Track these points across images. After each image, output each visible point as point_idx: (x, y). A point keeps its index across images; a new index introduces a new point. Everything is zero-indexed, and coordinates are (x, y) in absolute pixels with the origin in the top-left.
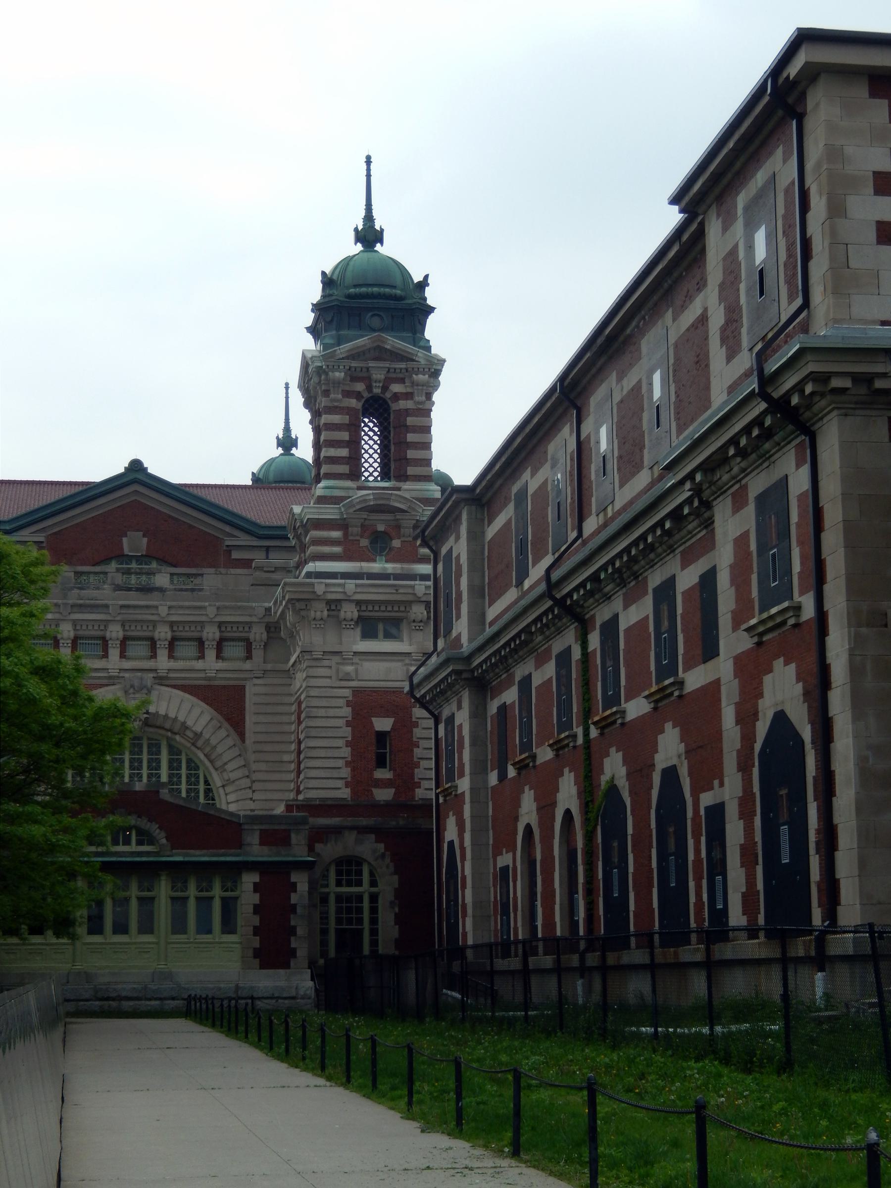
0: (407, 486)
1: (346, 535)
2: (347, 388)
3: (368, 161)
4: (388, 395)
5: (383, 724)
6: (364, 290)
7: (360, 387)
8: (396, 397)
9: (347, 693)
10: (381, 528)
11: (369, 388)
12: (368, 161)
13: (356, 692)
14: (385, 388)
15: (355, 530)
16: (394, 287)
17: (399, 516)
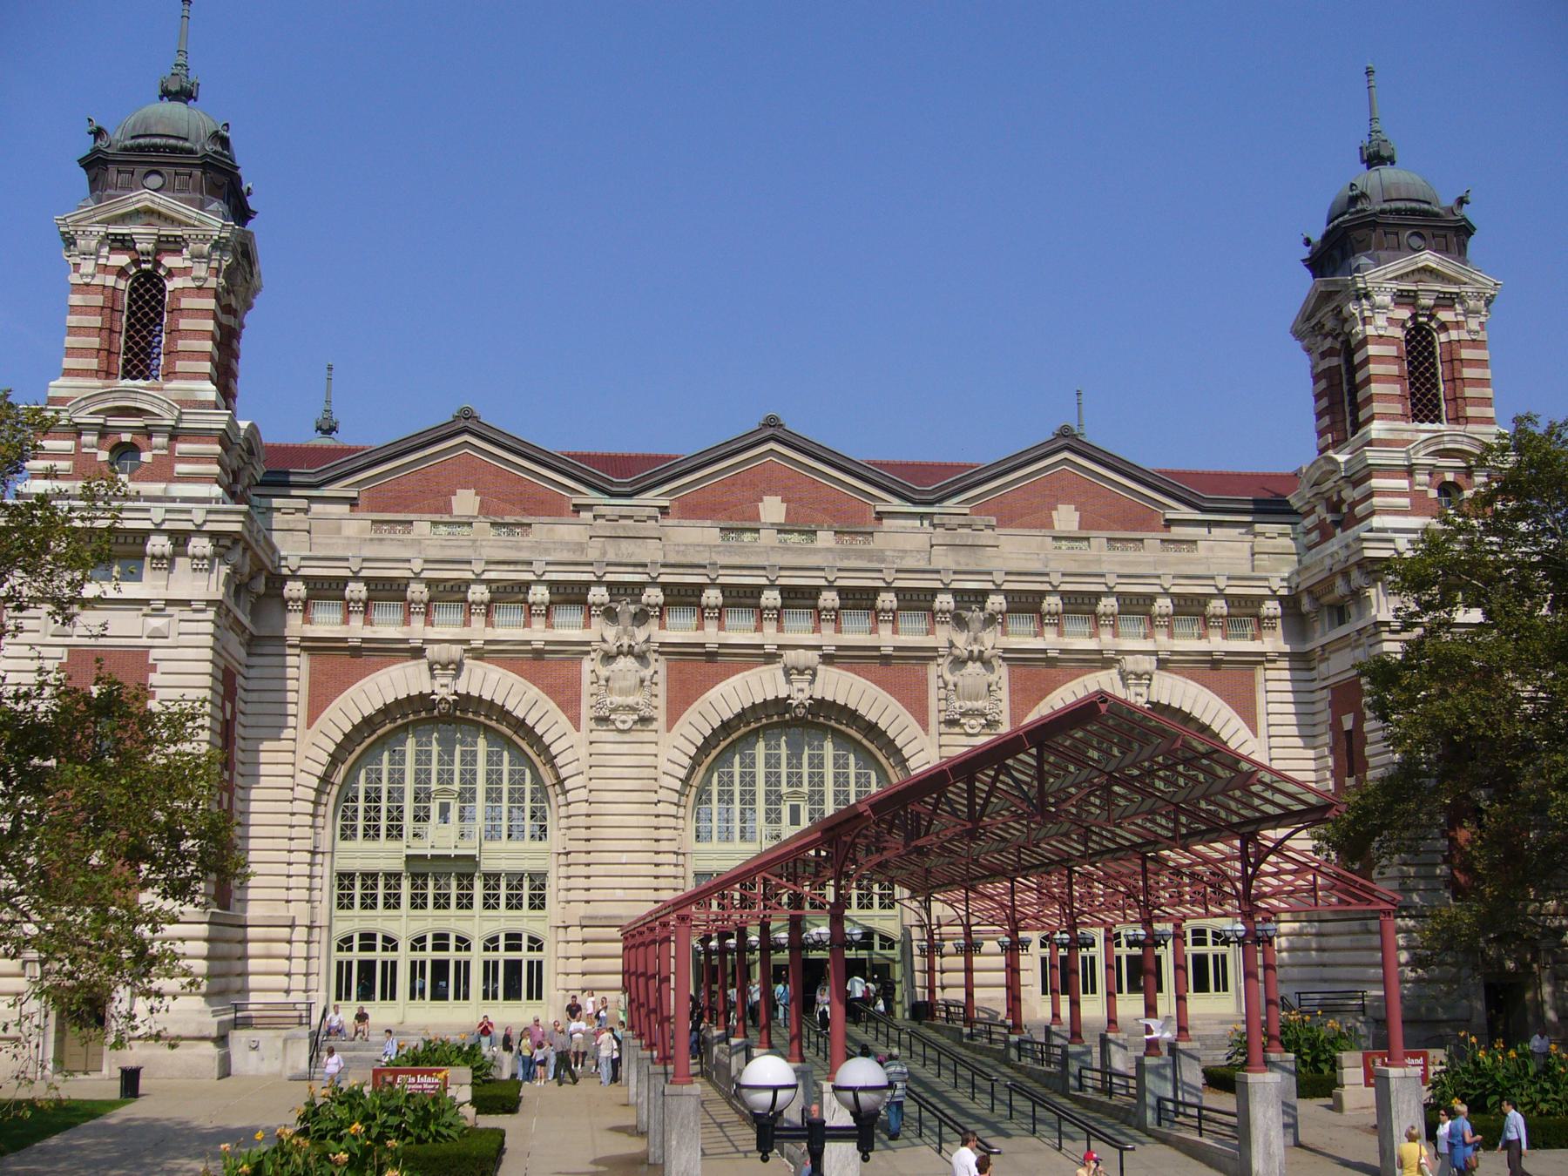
0: (175, 384)
1: (79, 446)
2: (102, 261)
6: (141, 141)
8: (171, 273)
10: (126, 437)
14: (158, 264)
16: (186, 139)
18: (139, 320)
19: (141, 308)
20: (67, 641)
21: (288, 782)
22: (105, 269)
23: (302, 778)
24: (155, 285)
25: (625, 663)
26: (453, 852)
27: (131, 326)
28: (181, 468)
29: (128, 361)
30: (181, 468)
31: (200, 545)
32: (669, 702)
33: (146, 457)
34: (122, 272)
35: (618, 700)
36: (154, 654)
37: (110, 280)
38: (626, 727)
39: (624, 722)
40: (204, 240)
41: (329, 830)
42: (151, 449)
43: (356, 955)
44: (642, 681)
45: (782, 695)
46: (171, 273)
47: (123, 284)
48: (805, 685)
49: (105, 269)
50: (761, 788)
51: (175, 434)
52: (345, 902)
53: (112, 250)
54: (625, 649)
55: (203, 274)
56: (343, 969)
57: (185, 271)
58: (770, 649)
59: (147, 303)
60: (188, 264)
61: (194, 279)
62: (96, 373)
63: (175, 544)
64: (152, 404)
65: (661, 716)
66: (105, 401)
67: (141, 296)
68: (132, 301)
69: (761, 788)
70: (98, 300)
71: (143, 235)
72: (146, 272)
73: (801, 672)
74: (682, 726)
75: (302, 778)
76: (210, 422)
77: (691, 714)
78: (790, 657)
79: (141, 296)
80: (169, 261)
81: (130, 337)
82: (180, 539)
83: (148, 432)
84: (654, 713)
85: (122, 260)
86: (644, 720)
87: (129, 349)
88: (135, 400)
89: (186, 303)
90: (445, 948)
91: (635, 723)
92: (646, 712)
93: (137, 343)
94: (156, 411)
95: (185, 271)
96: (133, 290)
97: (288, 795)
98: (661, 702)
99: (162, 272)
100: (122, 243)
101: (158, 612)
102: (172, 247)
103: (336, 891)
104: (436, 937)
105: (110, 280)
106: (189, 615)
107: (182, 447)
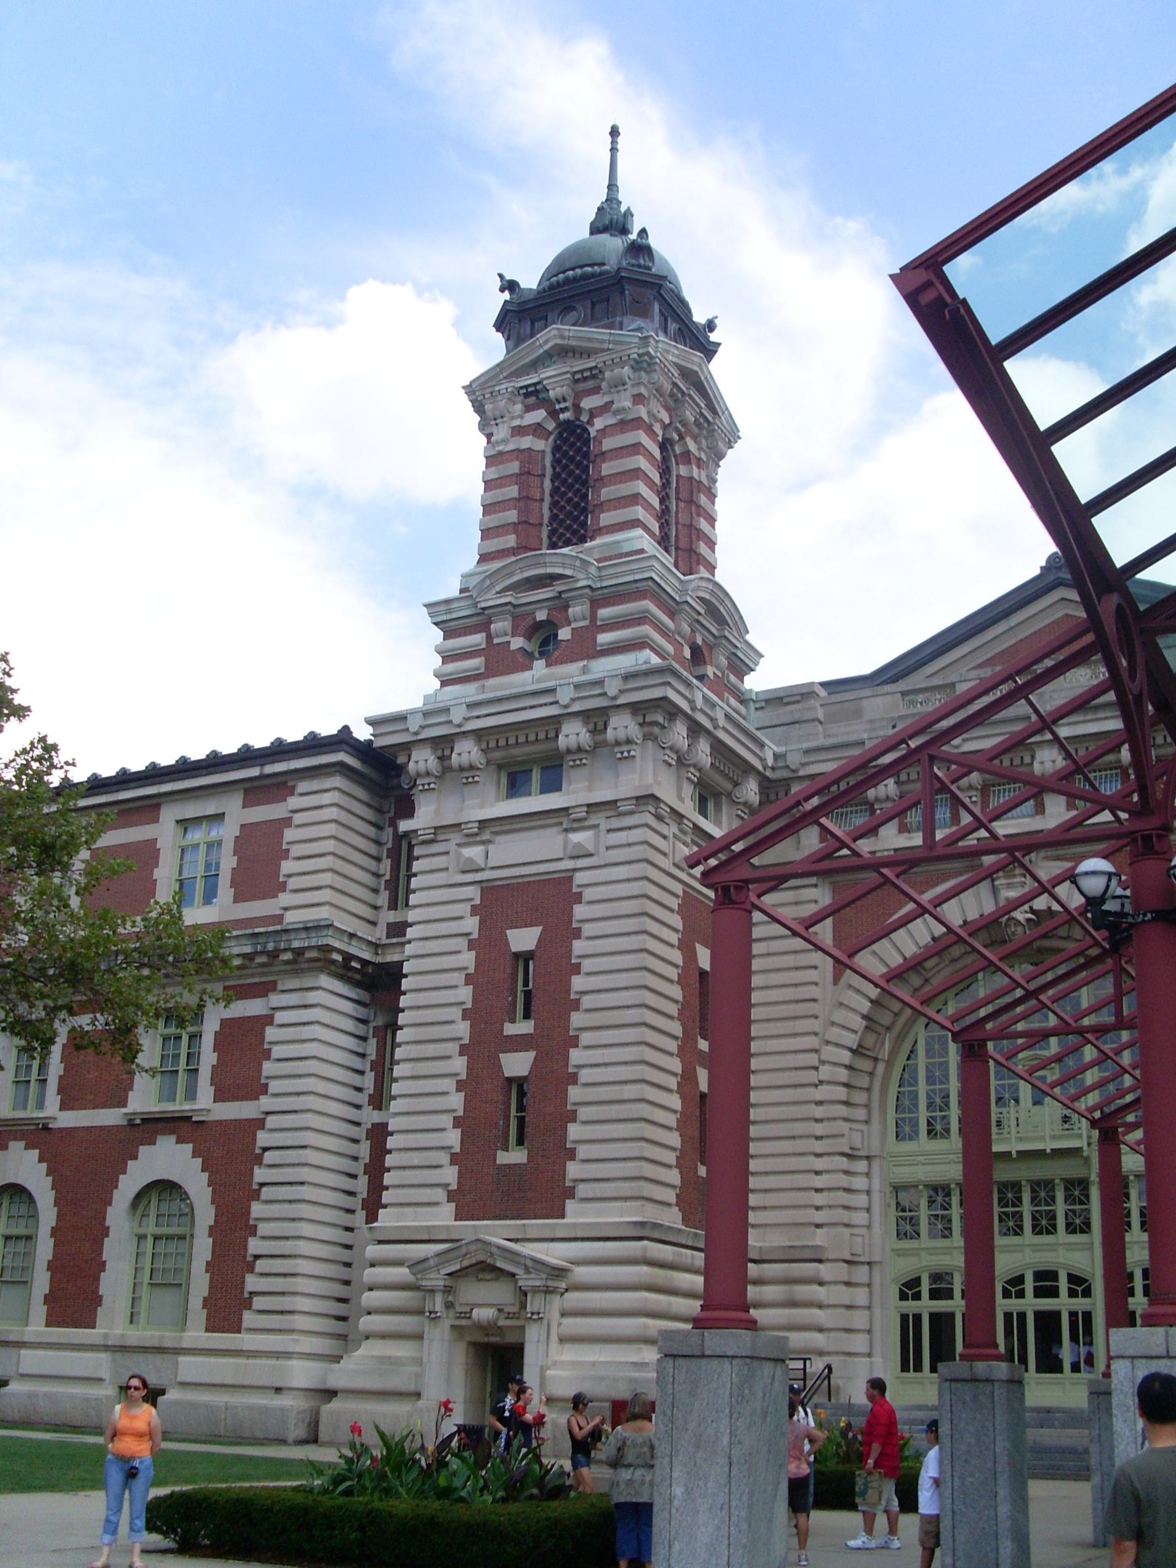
0: (599, 541)
1: (489, 638)
2: (517, 422)
3: (614, 132)
4: (584, 418)
5: (523, 939)
8: (593, 414)
9: (474, 893)
10: (541, 616)
11: (553, 414)
12: (614, 132)
13: (489, 890)
14: (577, 409)
15: (501, 625)
16: (604, 264)
17: (560, 587)
18: (564, 482)
19: (566, 467)
20: (479, 877)
21: (813, 1059)
22: (519, 431)
23: (829, 1052)
24: (579, 437)
26: (1049, 1146)
27: (555, 491)
28: (604, 638)
30: (604, 638)
31: (622, 726)
33: (564, 634)
34: (537, 430)
36: (580, 878)
37: (526, 442)
41: (876, 1125)
42: (569, 623)
43: (926, 1306)
46: (593, 414)
47: (540, 445)
49: (519, 431)
51: (600, 598)
52: (907, 1228)
53: (528, 409)
55: (627, 404)
56: (909, 1326)
57: (606, 408)
59: (572, 459)
60: (607, 399)
61: (616, 413)
62: (512, 551)
63: (594, 732)
64: (564, 566)
66: (510, 575)
67: (565, 454)
68: (556, 462)
70: (514, 467)
71: (555, 378)
72: (567, 422)
75: (829, 1052)
76: (633, 572)
79: (565, 454)
80: (588, 403)
81: (554, 504)
82: (596, 719)
83: (561, 604)
85: (539, 415)
87: (554, 517)
88: (545, 565)
89: (608, 444)
90: (1053, 1292)
93: (562, 508)
94: (568, 572)
95: (606, 408)
96: (556, 449)
97: (812, 1076)
99: (584, 418)
100: (534, 395)
101: (579, 825)
102: (590, 384)
103: (893, 1213)
104: (1039, 1275)
105: (526, 442)
106: (616, 823)
107: (604, 613)
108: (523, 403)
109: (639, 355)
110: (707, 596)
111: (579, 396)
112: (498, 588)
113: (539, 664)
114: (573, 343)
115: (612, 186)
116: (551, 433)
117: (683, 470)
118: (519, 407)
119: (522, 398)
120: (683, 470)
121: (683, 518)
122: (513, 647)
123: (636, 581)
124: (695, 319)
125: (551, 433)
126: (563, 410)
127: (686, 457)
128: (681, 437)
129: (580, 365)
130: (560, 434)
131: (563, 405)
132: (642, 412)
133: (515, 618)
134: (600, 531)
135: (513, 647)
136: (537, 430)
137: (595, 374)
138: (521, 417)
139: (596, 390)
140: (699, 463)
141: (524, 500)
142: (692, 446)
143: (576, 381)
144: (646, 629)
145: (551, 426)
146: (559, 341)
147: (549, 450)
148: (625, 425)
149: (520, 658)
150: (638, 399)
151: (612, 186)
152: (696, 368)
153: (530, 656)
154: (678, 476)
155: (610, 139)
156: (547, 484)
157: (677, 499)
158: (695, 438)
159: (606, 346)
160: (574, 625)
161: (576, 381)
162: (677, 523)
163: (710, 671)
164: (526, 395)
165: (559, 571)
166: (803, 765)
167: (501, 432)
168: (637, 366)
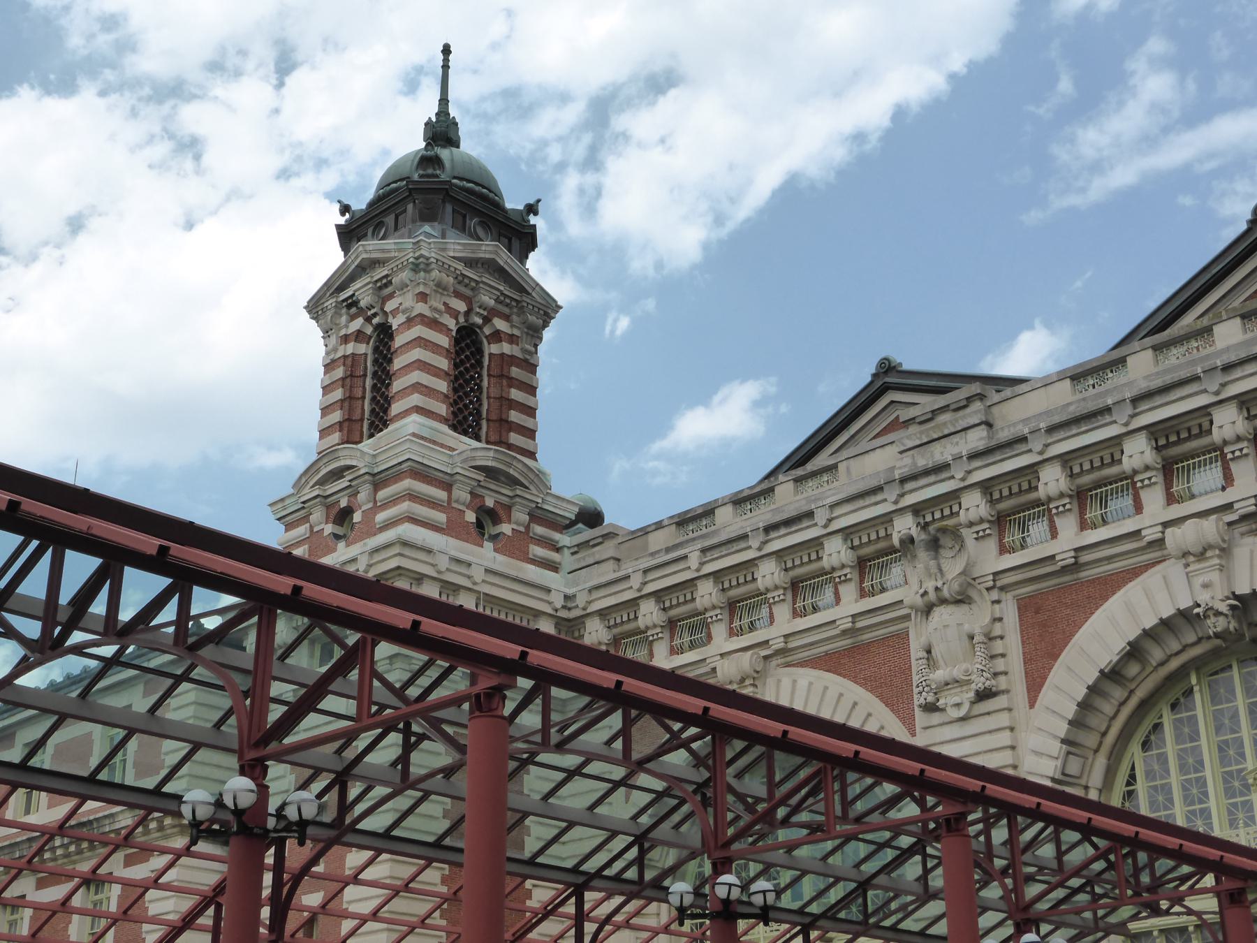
2: (343, 332)
3: (446, 50)
7: (358, 323)
10: (343, 503)
11: (368, 320)
15: (317, 515)
22: (345, 339)
25: (942, 615)
28: (381, 517)
29: (371, 424)
30: (381, 517)
32: (1027, 661)
33: (357, 517)
34: (359, 336)
35: (940, 675)
37: (350, 348)
38: (962, 712)
39: (958, 705)
40: (402, 270)
44: (972, 638)
45: (1185, 603)
47: (362, 348)
48: (1215, 576)
50: (1210, 773)
53: (353, 318)
54: (932, 596)
58: (1151, 534)
61: (404, 312)
65: (1017, 681)
66: (318, 470)
69: (1210, 773)
73: (1201, 556)
74: (1047, 695)
77: (1057, 674)
78: (1174, 537)
80: (389, 306)
83: (353, 492)
84: (1002, 683)
85: (358, 323)
86: (984, 695)
91: (973, 703)
92: (979, 683)
94: (354, 463)
96: (376, 349)
98: (1015, 662)
105: (350, 348)
107: (382, 494)
108: (348, 314)
109: (417, 258)
110: (490, 463)
111: (385, 300)
112: (311, 484)
113: (341, 545)
114: (374, 255)
115: (444, 101)
116: (370, 337)
117: (494, 349)
118: (344, 319)
119: (344, 310)
120: (494, 349)
121: (495, 392)
122: (326, 533)
123: (400, 464)
124: (509, 205)
125: (370, 337)
126: (375, 315)
127: (497, 336)
128: (487, 320)
129: (380, 273)
130: (378, 335)
131: (373, 311)
132: (421, 308)
133: (328, 507)
134: (392, 420)
135: (326, 533)
136: (359, 336)
137: (385, 283)
138: (347, 326)
139: (391, 296)
140: (512, 339)
141: (349, 400)
142: (500, 324)
143: (380, 288)
144: (405, 506)
145: (369, 330)
146: (365, 256)
147: (370, 352)
148: (410, 322)
149: (331, 541)
150: (423, 297)
151: (444, 101)
152: (492, 256)
153: (337, 537)
154: (490, 355)
155: (442, 57)
156: (369, 382)
157: (489, 375)
158: (507, 318)
159: (393, 254)
160: (364, 508)
161: (380, 288)
162: (488, 398)
163: (506, 528)
164: (349, 307)
165: (348, 462)
166: (590, 602)
167: (333, 340)
168: (416, 268)
